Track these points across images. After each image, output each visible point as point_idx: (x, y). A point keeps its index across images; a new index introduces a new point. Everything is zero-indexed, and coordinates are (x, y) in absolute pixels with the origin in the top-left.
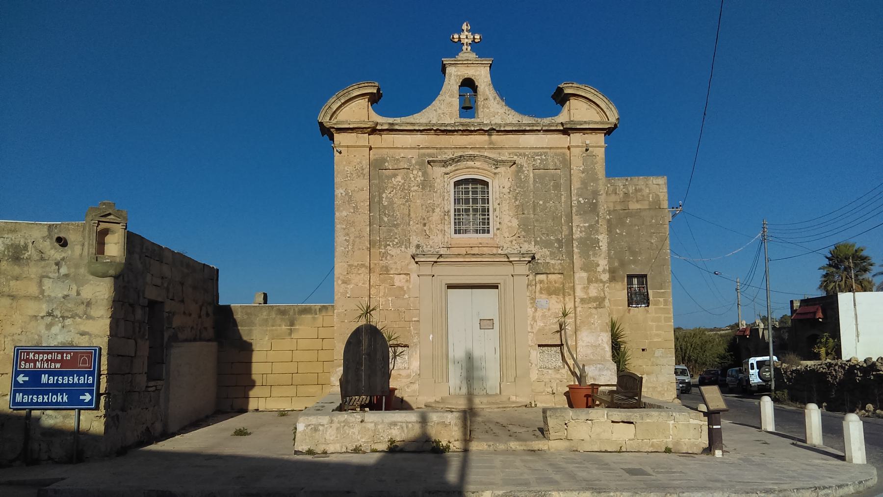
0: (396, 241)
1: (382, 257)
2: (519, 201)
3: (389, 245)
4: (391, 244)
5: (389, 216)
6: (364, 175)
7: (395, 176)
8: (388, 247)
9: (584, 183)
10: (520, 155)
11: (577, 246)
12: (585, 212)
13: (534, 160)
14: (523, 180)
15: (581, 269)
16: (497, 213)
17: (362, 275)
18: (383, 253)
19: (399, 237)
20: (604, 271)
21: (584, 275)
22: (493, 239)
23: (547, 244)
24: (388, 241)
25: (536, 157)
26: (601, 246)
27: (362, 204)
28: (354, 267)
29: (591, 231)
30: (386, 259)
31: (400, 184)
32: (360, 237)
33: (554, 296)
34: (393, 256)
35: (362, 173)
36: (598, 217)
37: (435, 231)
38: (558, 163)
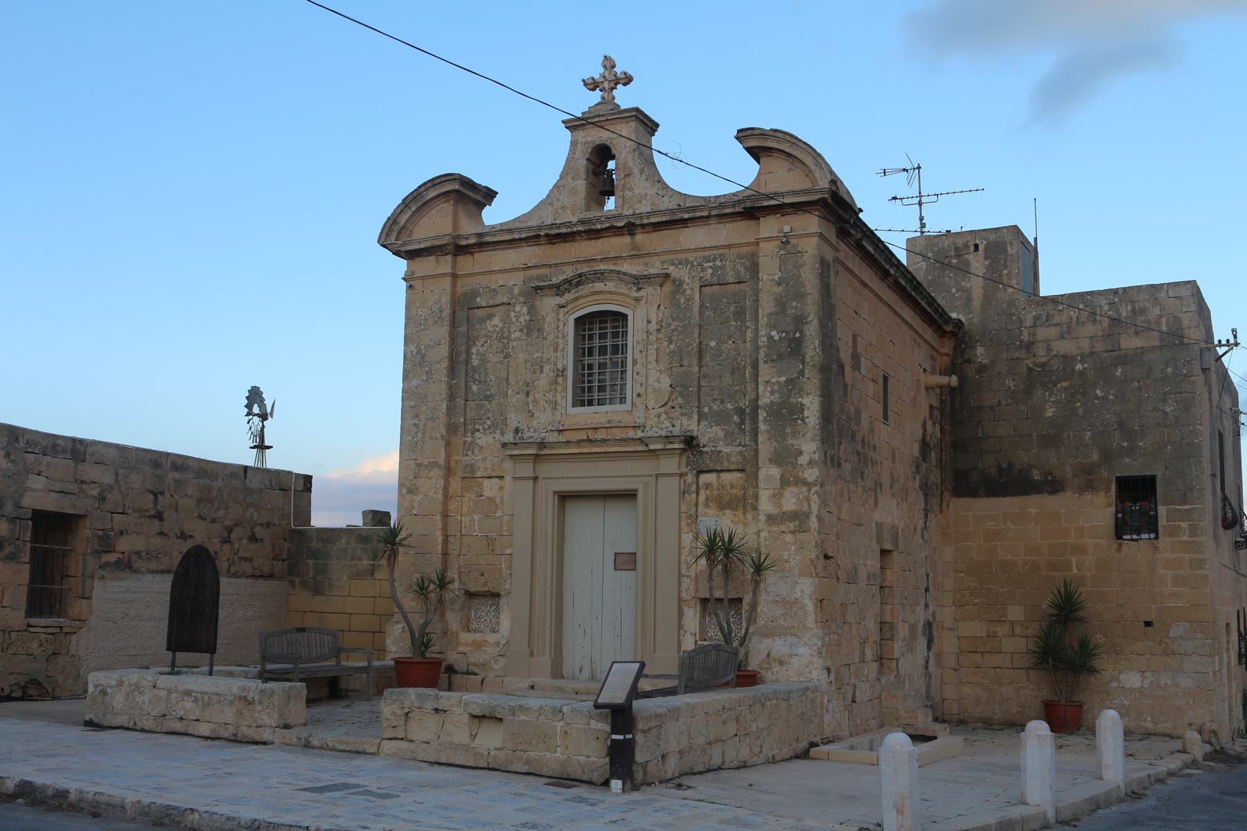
0: (489, 422)
1: (467, 451)
2: (674, 343)
3: (478, 430)
4: (481, 428)
5: (480, 382)
6: (443, 319)
7: (491, 317)
8: (477, 434)
9: (781, 305)
10: (680, 263)
11: (765, 420)
12: (781, 357)
13: (702, 270)
14: (682, 306)
15: (771, 461)
16: (639, 367)
17: (434, 479)
18: (470, 444)
19: (493, 416)
20: (811, 463)
21: (775, 471)
22: (630, 412)
23: (720, 418)
24: (477, 423)
25: (706, 265)
26: (808, 417)
27: (438, 366)
28: (423, 467)
29: (790, 391)
30: (473, 454)
31: (497, 329)
32: (432, 419)
33: (728, 512)
34: (482, 448)
35: (440, 317)
36: (803, 364)
37: (541, 404)
38: (742, 271)
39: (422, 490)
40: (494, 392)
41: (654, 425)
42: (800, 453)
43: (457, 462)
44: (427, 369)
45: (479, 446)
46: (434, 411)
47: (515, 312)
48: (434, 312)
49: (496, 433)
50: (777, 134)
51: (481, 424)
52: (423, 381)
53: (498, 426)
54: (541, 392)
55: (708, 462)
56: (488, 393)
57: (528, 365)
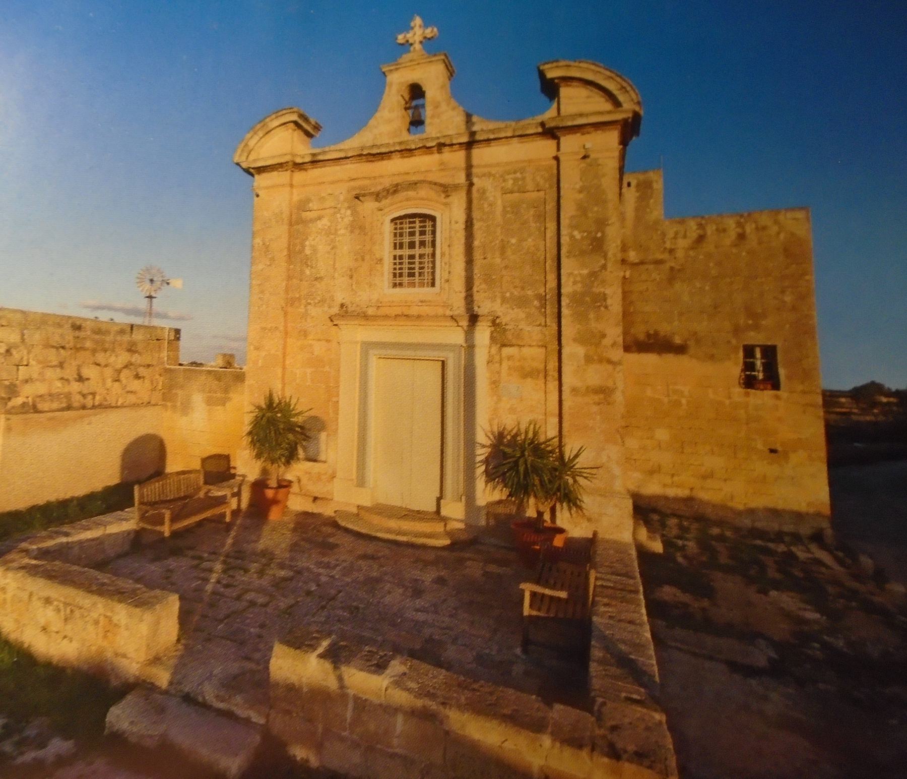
7: (320, 218)
9: (583, 210)
10: (484, 175)
11: (568, 306)
12: (583, 253)
13: (504, 181)
15: (575, 340)
16: (446, 259)
20: (614, 344)
21: (580, 351)
22: (440, 294)
23: (522, 302)
26: (611, 305)
29: (593, 282)
33: (529, 380)
36: (605, 259)
38: (542, 182)
47: (341, 214)
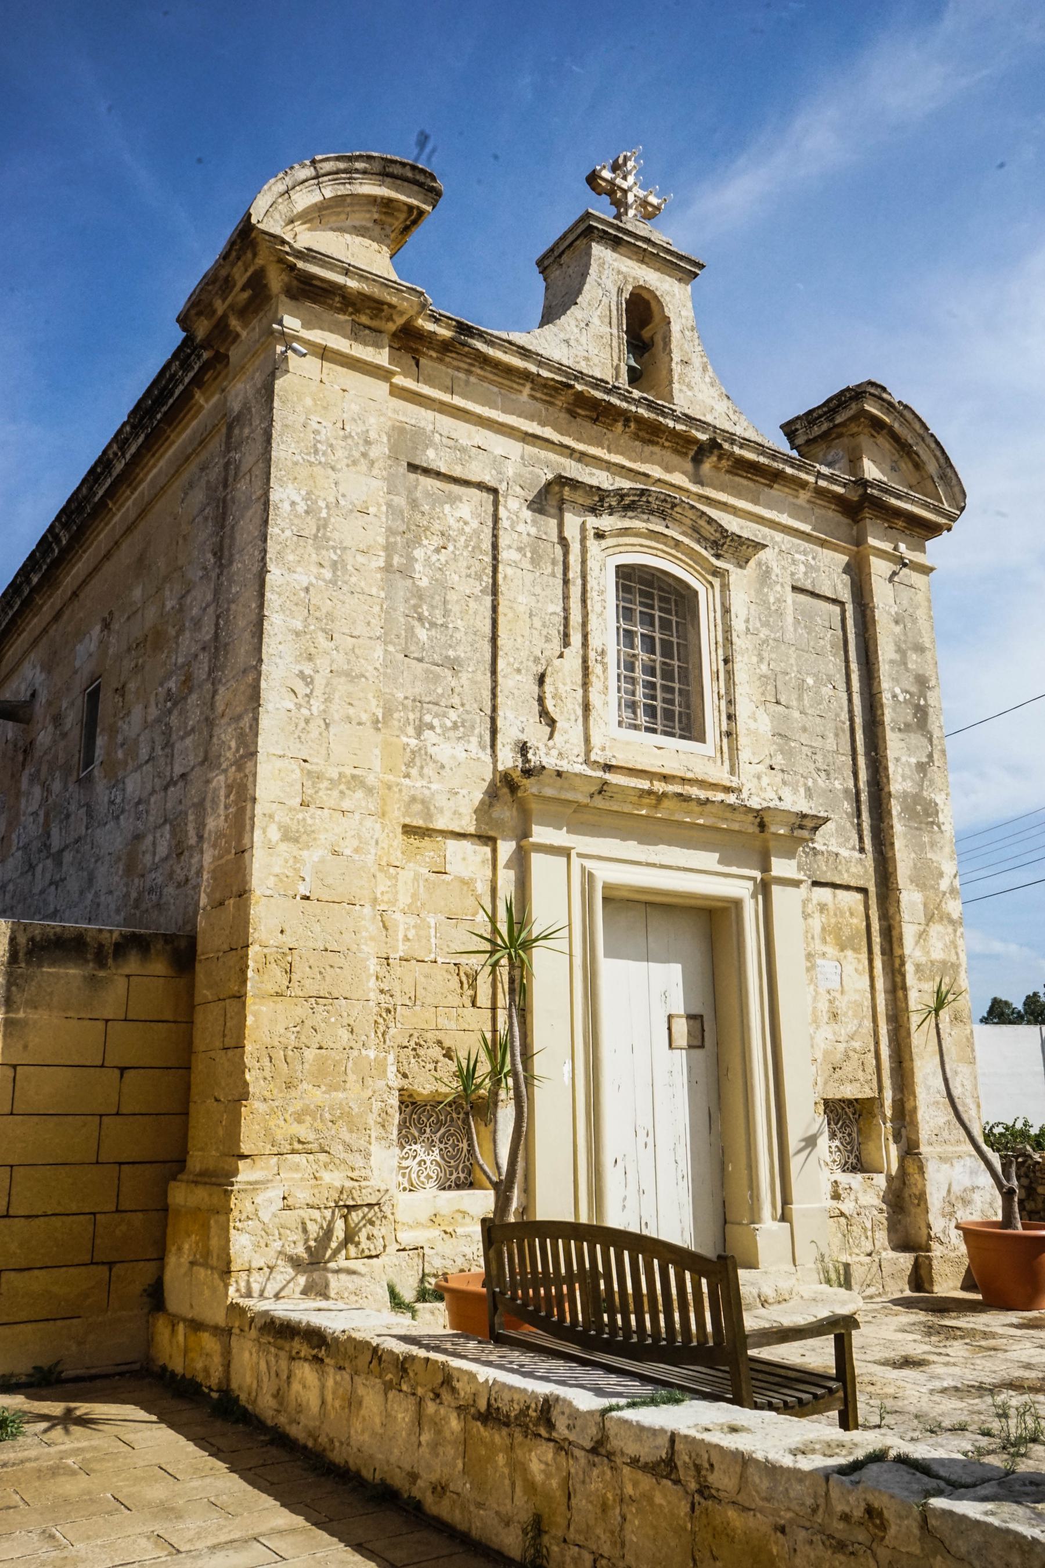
0: (453, 715)
1: (407, 765)
2: (766, 663)
3: (432, 727)
4: (436, 722)
5: (433, 625)
6: (372, 463)
8: (427, 734)
14: (773, 608)
17: (357, 816)
18: (413, 752)
19: (463, 705)
24: (429, 712)
25: (797, 556)
27: (361, 558)
28: (325, 784)
31: (467, 529)
32: (352, 677)
34: (443, 767)
35: (364, 455)
37: (570, 706)
39: (322, 837)
40: (462, 655)
41: (753, 791)
42: (941, 875)
43: (389, 788)
44: (335, 558)
45: (435, 762)
46: (353, 659)
47: (509, 511)
48: (350, 436)
49: (469, 742)
50: (906, 413)
51: (436, 715)
52: (324, 580)
53: (473, 727)
54: (568, 681)
55: (824, 868)
56: (451, 653)
57: (537, 622)
